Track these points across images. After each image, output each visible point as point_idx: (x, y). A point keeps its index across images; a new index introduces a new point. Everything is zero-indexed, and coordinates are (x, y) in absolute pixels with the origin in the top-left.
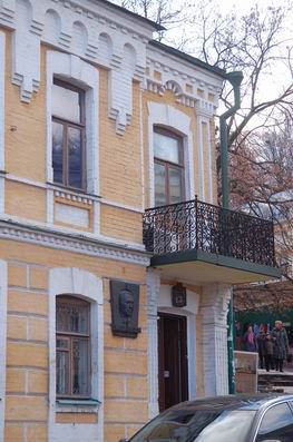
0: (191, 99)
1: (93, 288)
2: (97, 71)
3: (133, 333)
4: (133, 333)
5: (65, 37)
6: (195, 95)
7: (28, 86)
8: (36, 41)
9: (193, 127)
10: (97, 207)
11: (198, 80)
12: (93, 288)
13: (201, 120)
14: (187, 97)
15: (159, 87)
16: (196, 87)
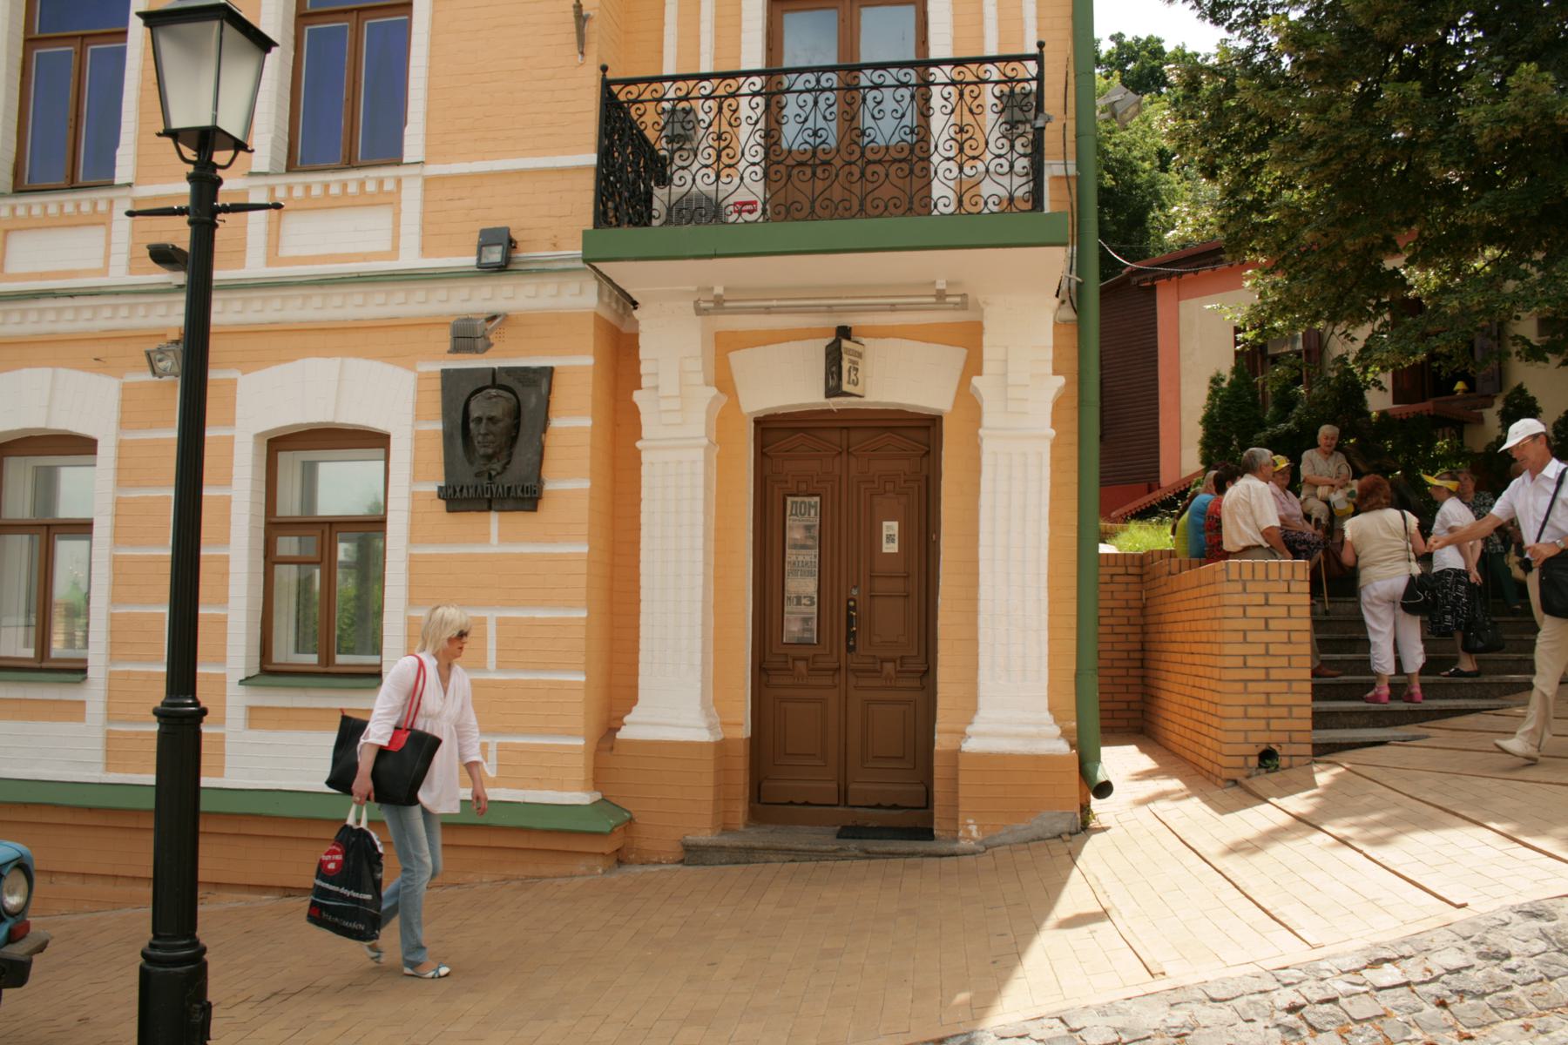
3: (524, 496)
4: (524, 496)
10: (412, 196)
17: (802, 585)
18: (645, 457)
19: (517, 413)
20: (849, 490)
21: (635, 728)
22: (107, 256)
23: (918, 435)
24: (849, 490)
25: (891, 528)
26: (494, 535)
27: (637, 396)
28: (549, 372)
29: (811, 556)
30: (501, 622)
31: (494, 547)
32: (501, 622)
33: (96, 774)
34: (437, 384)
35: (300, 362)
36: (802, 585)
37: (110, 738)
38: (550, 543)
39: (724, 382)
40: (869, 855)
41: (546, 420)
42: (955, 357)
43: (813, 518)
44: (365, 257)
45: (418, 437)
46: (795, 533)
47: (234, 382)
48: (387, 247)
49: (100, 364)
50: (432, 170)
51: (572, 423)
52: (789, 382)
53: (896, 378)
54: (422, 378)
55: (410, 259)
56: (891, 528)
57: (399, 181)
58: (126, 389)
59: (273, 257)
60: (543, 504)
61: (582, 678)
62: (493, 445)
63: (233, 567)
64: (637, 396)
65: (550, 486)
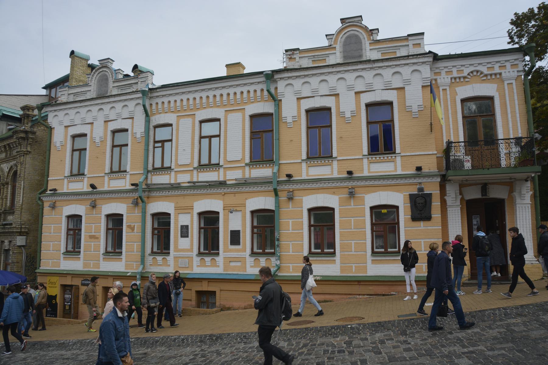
0: (496, 74)
1: (398, 198)
2: (395, 91)
3: (428, 218)
4: (428, 218)
5: (370, 84)
6: (497, 70)
7: (348, 115)
8: (353, 93)
9: (501, 91)
11: (497, 62)
12: (398, 198)
13: (506, 83)
14: (491, 75)
15: (465, 77)
16: (497, 66)
18: (448, 209)
19: (426, 202)
22: (332, 171)
26: (422, 225)
27: (446, 197)
32: (424, 242)
33: (339, 274)
34: (408, 196)
35: (378, 193)
37: (341, 267)
39: (461, 193)
40: (501, 284)
41: (431, 204)
43: (478, 219)
44: (390, 172)
45: (404, 207)
46: (475, 222)
48: (393, 169)
49: (334, 193)
50: (402, 154)
51: (436, 204)
52: (474, 194)
53: (496, 193)
55: (399, 172)
57: (395, 157)
58: (340, 198)
59: (369, 172)
62: (421, 208)
63: (367, 233)
64: (446, 197)
65: (432, 216)
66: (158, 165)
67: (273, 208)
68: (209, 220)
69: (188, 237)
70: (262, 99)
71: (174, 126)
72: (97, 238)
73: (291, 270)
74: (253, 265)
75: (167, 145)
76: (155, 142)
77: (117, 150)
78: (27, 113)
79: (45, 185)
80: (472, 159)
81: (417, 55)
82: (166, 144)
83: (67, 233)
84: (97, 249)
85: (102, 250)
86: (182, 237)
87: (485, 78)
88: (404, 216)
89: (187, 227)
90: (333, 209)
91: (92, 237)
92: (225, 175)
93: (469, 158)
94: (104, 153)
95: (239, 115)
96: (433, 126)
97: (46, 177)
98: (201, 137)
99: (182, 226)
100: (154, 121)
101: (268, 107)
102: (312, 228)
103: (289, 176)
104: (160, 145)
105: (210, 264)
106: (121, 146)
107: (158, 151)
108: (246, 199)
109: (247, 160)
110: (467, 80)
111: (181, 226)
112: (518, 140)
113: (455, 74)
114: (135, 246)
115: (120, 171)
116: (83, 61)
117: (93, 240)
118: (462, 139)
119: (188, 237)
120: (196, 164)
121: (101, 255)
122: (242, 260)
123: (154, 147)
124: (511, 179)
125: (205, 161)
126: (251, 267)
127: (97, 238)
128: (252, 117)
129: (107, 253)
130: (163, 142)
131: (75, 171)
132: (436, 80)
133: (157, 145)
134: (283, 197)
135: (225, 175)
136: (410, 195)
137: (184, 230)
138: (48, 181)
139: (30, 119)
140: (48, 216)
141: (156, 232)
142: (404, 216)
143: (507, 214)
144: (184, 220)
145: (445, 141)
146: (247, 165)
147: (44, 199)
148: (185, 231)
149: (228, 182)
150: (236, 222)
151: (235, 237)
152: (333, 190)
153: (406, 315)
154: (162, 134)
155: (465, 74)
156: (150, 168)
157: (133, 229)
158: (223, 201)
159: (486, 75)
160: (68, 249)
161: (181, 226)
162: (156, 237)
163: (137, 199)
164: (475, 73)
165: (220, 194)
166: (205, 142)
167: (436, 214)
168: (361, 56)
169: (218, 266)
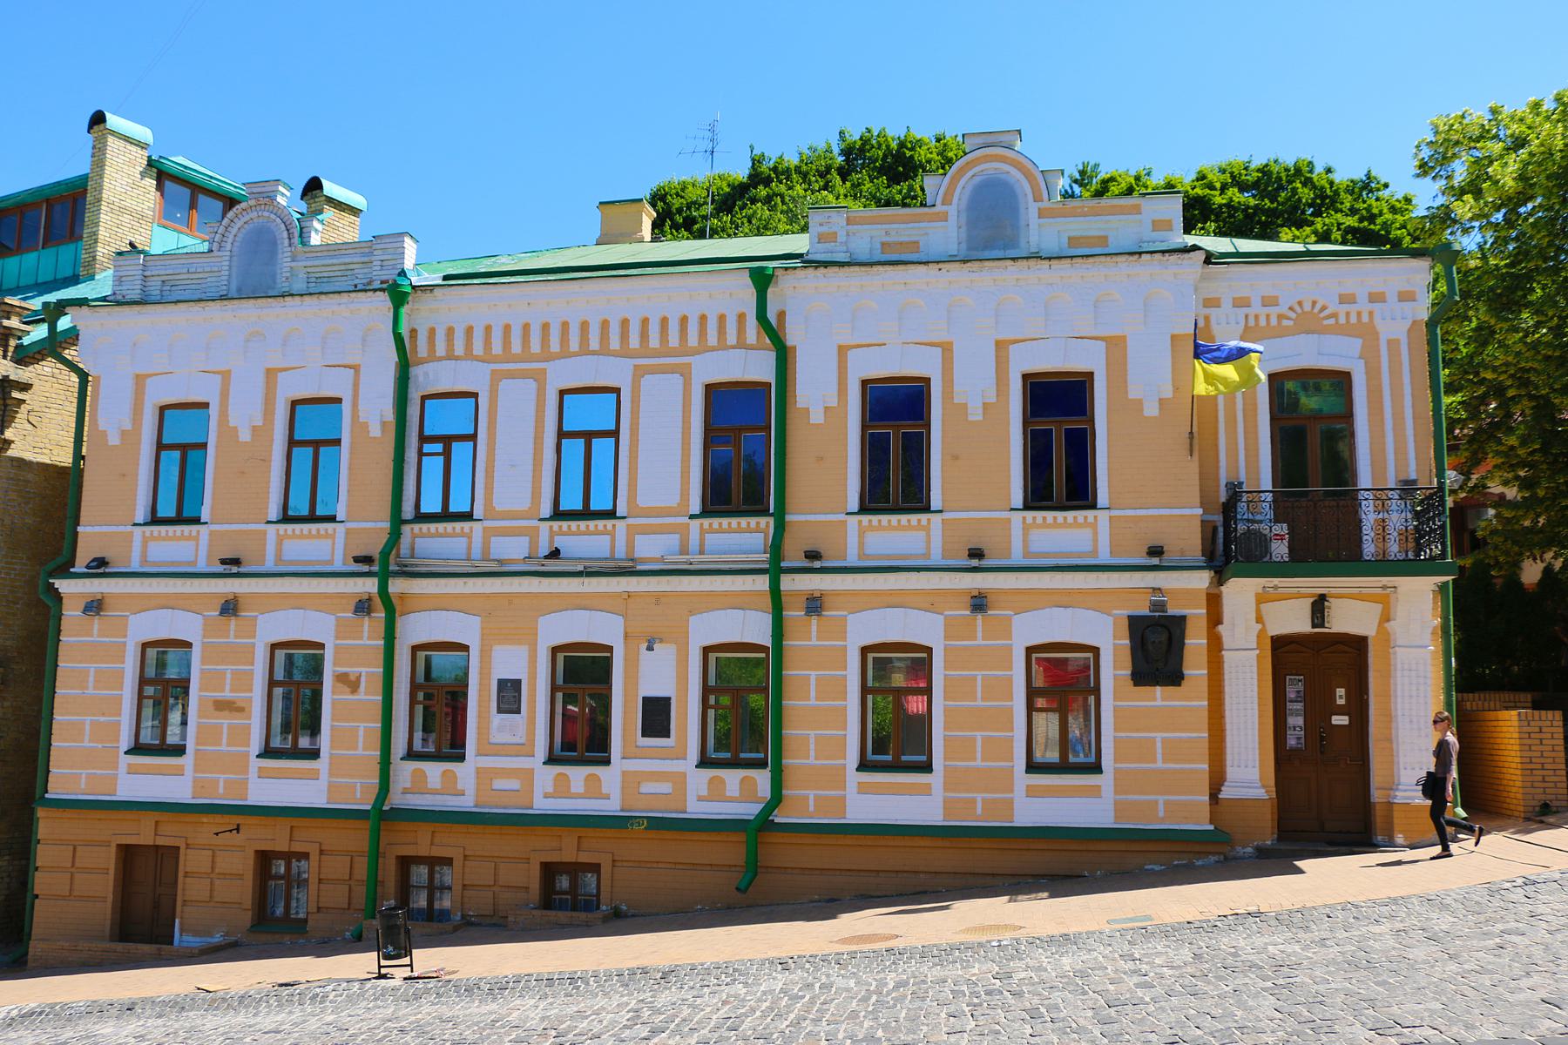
2: (1102, 345)
9: (1370, 356)
15: (1281, 317)
17: (1296, 720)
20: (1321, 672)
21: (1226, 793)
23: (1358, 645)
24: (1321, 672)
25: (1341, 692)
26: (1158, 697)
27: (1220, 628)
28: (1183, 618)
29: (1300, 706)
30: (1164, 740)
31: (1159, 703)
32: (1164, 740)
36: (1296, 720)
38: (1188, 699)
39: (1259, 619)
42: (1377, 609)
43: (1300, 686)
44: (1080, 555)
46: (1291, 693)
47: (1009, 618)
49: (931, 608)
51: (1195, 642)
52: (1293, 619)
53: (1348, 618)
54: (1116, 618)
56: (1341, 692)
60: (1184, 683)
61: (1206, 766)
66: (432, 504)
67: (767, 641)
68: (583, 672)
69: (518, 712)
70: (741, 344)
71: (483, 401)
72: (241, 710)
73: (811, 808)
74: (705, 793)
75: (460, 450)
76: (424, 439)
77: (303, 456)
78: (6, 323)
79: (66, 552)
80: (1291, 532)
81: (1163, 252)
82: (455, 446)
83: (140, 691)
84: (242, 735)
85: (256, 745)
86: (500, 711)
87: (1332, 321)
88: (1113, 671)
89: (516, 684)
90: (929, 650)
91: (223, 706)
92: (630, 544)
93: (1282, 529)
94: (266, 461)
95: (677, 379)
96: (1196, 441)
97: (69, 523)
98: (562, 434)
99: (502, 684)
100: (421, 379)
101: (758, 367)
102: (870, 697)
103: (813, 555)
104: (439, 447)
105: (582, 790)
106: (316, 444)
107: (433, 467)
108: (691, 613)
109: (695, 506)
110: (1285, 323)
111: (500, 681)
112: (1407, 489)
113: (1256, 308)
114: (361, 733)
115: (312, 518)
116: (134, 148)
117: (226, 713)
118: (1266, 483)
119: (518, 712)
120: (546, 509)
121: (253, 758)
122: (680, 780)
123: (421, 454)
124: (1384, 587)
125: (572, 501)
126: (700, 799)
127: (241, 710)
128: (710, 389)
129: (268, 752)
130: (447, 440)
131: (167, 509)
132: (1207, 319)
133: (427, 448)
134: (794, 613)
135: (630, 544)
136: (1130, 617)
137: (509, 694)
138: (76, 534)
139: (13, 343)
140: (78, 640)
141: (421, 696)
142: (1113, 671)
143: (1371, 674)
144: (509, 662)
145: (1223, 483)
146: (692, 517)
147: (63, 586)
148: (509, 695)
149: (639, 567)
150: (658, 671)
151: (656, 717)
152: (930, 602)
153: (1131, 920)
154: (443, 420)
155: (1283, 309)
156: (408, 511)
157: (354, 686)
158: (625, 616)
159: (1334, 315)
160: (142, 740)
161: (500, 681)
162: (419, 709)
163: (370, 599)
164: (1307, 307)
165: (618, 595)
166: (574, 448)
167: (1195, 668)
168: (1013, 242)
169: (607, 797)
